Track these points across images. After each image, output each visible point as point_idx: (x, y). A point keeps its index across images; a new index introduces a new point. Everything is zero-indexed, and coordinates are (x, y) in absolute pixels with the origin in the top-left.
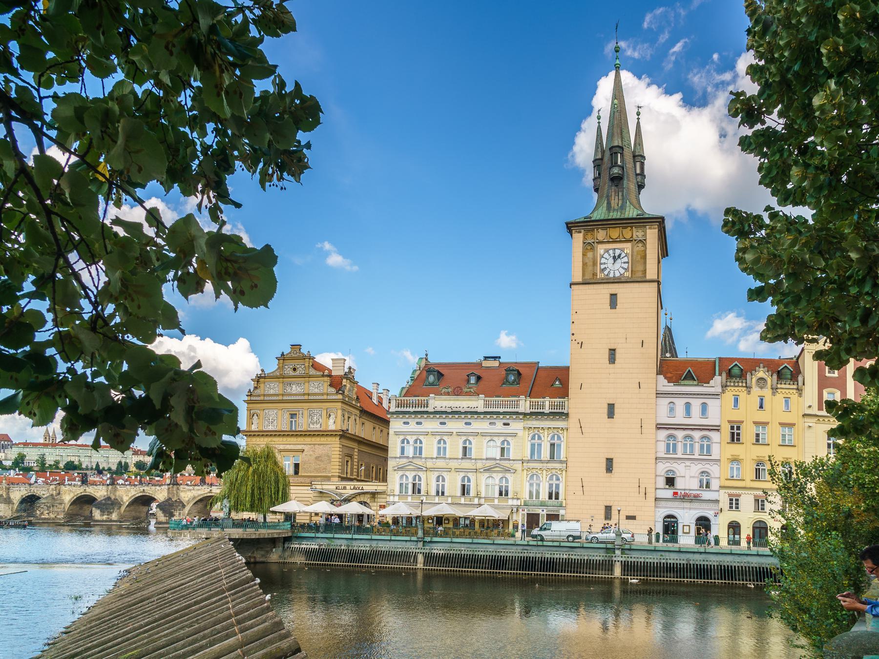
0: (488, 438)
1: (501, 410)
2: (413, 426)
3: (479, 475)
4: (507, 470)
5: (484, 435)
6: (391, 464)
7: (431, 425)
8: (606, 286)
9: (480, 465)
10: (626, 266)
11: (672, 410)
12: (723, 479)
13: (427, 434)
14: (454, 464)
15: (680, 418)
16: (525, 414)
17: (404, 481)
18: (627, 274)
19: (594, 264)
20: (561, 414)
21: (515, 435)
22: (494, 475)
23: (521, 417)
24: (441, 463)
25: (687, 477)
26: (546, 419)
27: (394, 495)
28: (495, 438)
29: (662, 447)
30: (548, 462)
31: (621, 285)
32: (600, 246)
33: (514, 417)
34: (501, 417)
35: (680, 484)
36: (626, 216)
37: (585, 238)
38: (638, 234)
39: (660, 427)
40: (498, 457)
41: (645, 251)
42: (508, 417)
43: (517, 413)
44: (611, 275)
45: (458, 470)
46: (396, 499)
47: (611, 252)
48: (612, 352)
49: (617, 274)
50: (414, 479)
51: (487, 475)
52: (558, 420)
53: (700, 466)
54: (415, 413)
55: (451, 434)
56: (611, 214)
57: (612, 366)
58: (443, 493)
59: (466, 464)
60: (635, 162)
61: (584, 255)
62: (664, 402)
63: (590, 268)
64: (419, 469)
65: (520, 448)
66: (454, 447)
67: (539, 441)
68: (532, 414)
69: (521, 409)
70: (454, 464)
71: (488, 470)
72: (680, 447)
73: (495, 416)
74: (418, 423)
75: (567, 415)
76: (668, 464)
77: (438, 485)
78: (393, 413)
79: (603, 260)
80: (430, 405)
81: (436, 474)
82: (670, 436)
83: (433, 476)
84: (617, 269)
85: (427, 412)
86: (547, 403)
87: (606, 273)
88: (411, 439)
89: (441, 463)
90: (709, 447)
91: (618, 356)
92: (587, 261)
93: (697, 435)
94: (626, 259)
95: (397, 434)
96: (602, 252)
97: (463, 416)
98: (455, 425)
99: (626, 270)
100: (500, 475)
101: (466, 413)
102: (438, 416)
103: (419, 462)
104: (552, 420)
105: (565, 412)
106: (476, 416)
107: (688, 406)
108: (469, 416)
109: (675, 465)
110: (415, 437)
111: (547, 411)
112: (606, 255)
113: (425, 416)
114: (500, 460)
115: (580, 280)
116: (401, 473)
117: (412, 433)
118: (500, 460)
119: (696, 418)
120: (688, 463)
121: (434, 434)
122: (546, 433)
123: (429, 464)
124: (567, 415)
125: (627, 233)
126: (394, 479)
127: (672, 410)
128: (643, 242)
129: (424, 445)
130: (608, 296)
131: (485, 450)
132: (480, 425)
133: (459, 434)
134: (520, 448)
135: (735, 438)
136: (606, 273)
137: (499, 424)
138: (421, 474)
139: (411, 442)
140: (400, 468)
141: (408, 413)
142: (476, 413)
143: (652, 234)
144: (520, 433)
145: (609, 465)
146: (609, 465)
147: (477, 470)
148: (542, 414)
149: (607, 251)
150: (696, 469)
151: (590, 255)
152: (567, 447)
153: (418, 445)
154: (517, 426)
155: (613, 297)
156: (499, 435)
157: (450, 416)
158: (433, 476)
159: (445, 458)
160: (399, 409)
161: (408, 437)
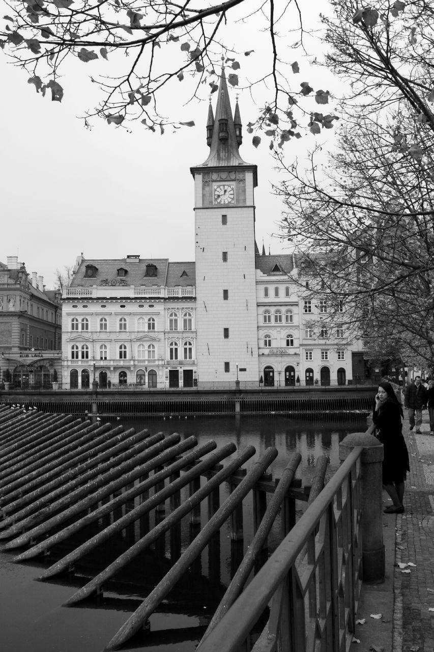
1: (147, 296)
2: (80, 309)
3: (133, 343)
4: (154, 340)
5: (135, 314)
6: (64, 337)
7: (94, 308)
8: (219, 210)
9: (133, 336)
10: (232, 196)
11: (266, 294)
12: (301, 339)
13: (92, 314)
14: (113, 336)
15: (272, 298)
16: (165, 299)
17: (75, 350)
18: (233, 202)
19: (211, 195)
20: (191, 298)
21: (158, 314)
22: (144, 343)
23: (162, 301)
24: (103, 336)
25: (279, 339)
26: (180, 302)
27: (68, 361)
28: (144, 317)
29: (261, 319)
30: (183, 332)
31: (229, 209)
32: (214, 184)
33: (157, 301)
34: (148, 301)
35: (274, 344)
36: (231, 165)
37: (203, 178)
39: (259, 305)
40: (146, 329)
41: (244, 187)
42: (153, 301)
43: (159, 298)
44: (222, 203)
45: (116, 341)
46: (69, 363)
47: (222, 187)
48: (225, 255)
49: (227, 202)
50: (83, 348)
51: (138, 343)
52: (188, 302)
53: (287, 331)
54: (82, 299)
55: (111, 314)
56: (221, 162)
57: (225, 263)
58: (105, 358)
59: (123, 336)
60: (235, 128)
61: (203, 189)
62: (262, 288)
63: (207, 198)
64: (87, 340)
65: (162, 324)
66: (113, 324)
67: (176, 318)
68: (169, 298)
69: (161, 296)
70: (113, 336)
71: (139, 340)
72: (273, 318)
73: (143, 301)
74: (84, 306)
75: (195, 298)
76: (266, 331)
77: (101, 352)
78: (64, 299)
79: (216, 193)
80: (93, 293)
81: (100, 344)
82: (267, 311)
83: (98, 345)
84: (226, 199)
85: (91, 298)
86: (180, 291)
87: (219, 201)
89: (103, 336)
90: (291, 316)
91: (229, 256)
92: (205, 193)
93: (283, 309)
94: (232, 192)
95: (68, 314)
96: (216, 187)
97: (119, 301)
98: (114, 308)
99: (233, 199)
100: (149, 343)
101: (121, 298)
102: (100, 301)
103: (86, 335)
104: (184, 302)
106: (129, 301)
107: (277, 290)
108: (124, 301)
109: (271, 331)
110: (82, 317)
111: (180, 296)
112: (218, 189)
113: (90, 301)
114: (148, 332)
115: (200, 205)
116: (72, 344)
117: (80, 314)
118: (148, 332)
119: (282, 298)
120: (279, 329)
121: (97, 314)
122: (180, 311)
123: (95, 337)
124: (195, 298)
125: (233, 176)
126: (66, 350)
127: (266, 294)
128: (243, 180)
129: (89, 323)
130: (221, 217)
131: (136, 325)
132: (132, 308)
133: (116, 314)
134: (162, 324)
136: (219, 201)
138: (88, 344)
139: (80, 320)
140: (72, 340)
141: (77, 299)
142: (129, 298)
143: (249, 176)
144: (162, 313)
145: (226, 333)
146: (226, 333)
147: (131, 341)
148: (177, 298)
149: (219, 186)
150: (284, 334)
151: (207, 189)
153: (85, 322)
154: (159, 307)
155: (224, 217)
156: (146, 314)
157: (110, 301)
158: (98, 345)
159: (106, 332)
160: (69, 296)
161: (77, 317)
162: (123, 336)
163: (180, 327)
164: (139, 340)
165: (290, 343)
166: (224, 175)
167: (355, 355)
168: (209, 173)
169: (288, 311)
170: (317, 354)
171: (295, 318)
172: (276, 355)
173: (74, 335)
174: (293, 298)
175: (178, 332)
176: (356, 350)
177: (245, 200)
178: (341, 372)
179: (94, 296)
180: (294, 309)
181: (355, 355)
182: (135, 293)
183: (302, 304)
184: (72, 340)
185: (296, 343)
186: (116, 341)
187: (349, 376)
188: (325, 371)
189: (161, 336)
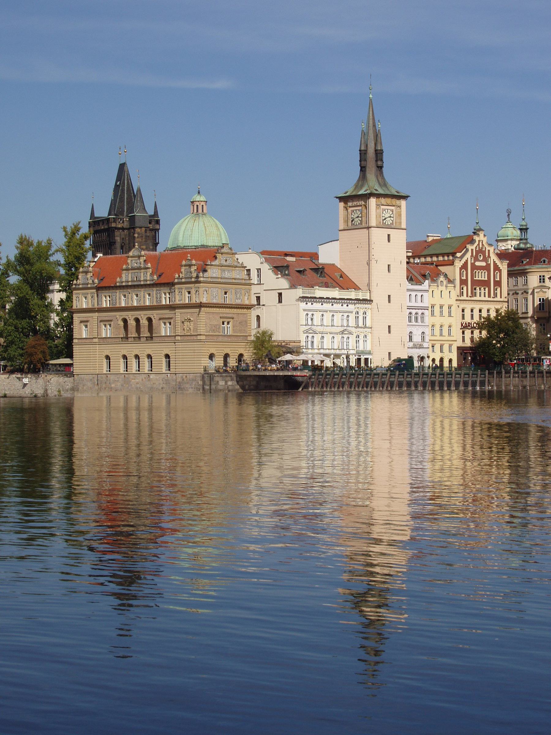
0: (342, 314)
4: (351, 333)
7: (317, 306)
15: (413, 304)
38: (398, 202)
79: (383, 215)
82: (410, 313)
85: (315, 298)
88: (310, 313)
91: (391, 268)
93: (420, 312)
98: (327, 306)
100: (347, 336)
105: (369, 299)
115: (374, 225)
116: (306, 335)
119: (419, 304)
124: (372, 301)
128: (400, 207)
132: (337, 307)
135: (433, 314)
137: (345, 305)
152: (372, 319)
154: (351, 307)
155: (389, 235)
162: (333, 329)
163: (361, 324)
164: (342, 332)
165: (423, 339)
166: (389, 200)
167: (458, 348)
168: (379, 198)
169: (423, 314)
170: (437, 348)
171: (426, 319)
172: (416, 348)
173: (308, 327)
174: (426, 304)
175: (361, 328)
176: (459, 345)
177: (400, 223)
178: (450, 361)
179: (318, 296)
180: (426, 312)
181: (458, 348)
182: (340, 294)
183: (430, 309)
184: (306, 332)
185: (427, 339)
186: (331, 333)
187: (455, 364)
188: (442, 360)
189: (353, 330)
